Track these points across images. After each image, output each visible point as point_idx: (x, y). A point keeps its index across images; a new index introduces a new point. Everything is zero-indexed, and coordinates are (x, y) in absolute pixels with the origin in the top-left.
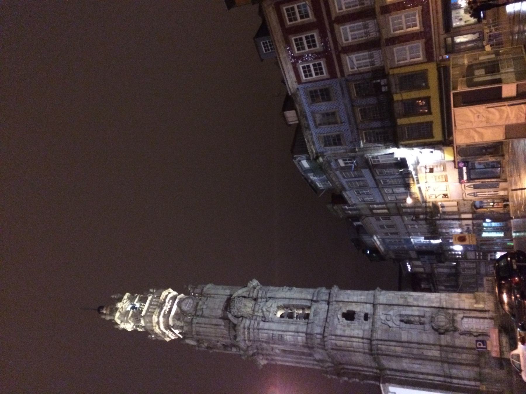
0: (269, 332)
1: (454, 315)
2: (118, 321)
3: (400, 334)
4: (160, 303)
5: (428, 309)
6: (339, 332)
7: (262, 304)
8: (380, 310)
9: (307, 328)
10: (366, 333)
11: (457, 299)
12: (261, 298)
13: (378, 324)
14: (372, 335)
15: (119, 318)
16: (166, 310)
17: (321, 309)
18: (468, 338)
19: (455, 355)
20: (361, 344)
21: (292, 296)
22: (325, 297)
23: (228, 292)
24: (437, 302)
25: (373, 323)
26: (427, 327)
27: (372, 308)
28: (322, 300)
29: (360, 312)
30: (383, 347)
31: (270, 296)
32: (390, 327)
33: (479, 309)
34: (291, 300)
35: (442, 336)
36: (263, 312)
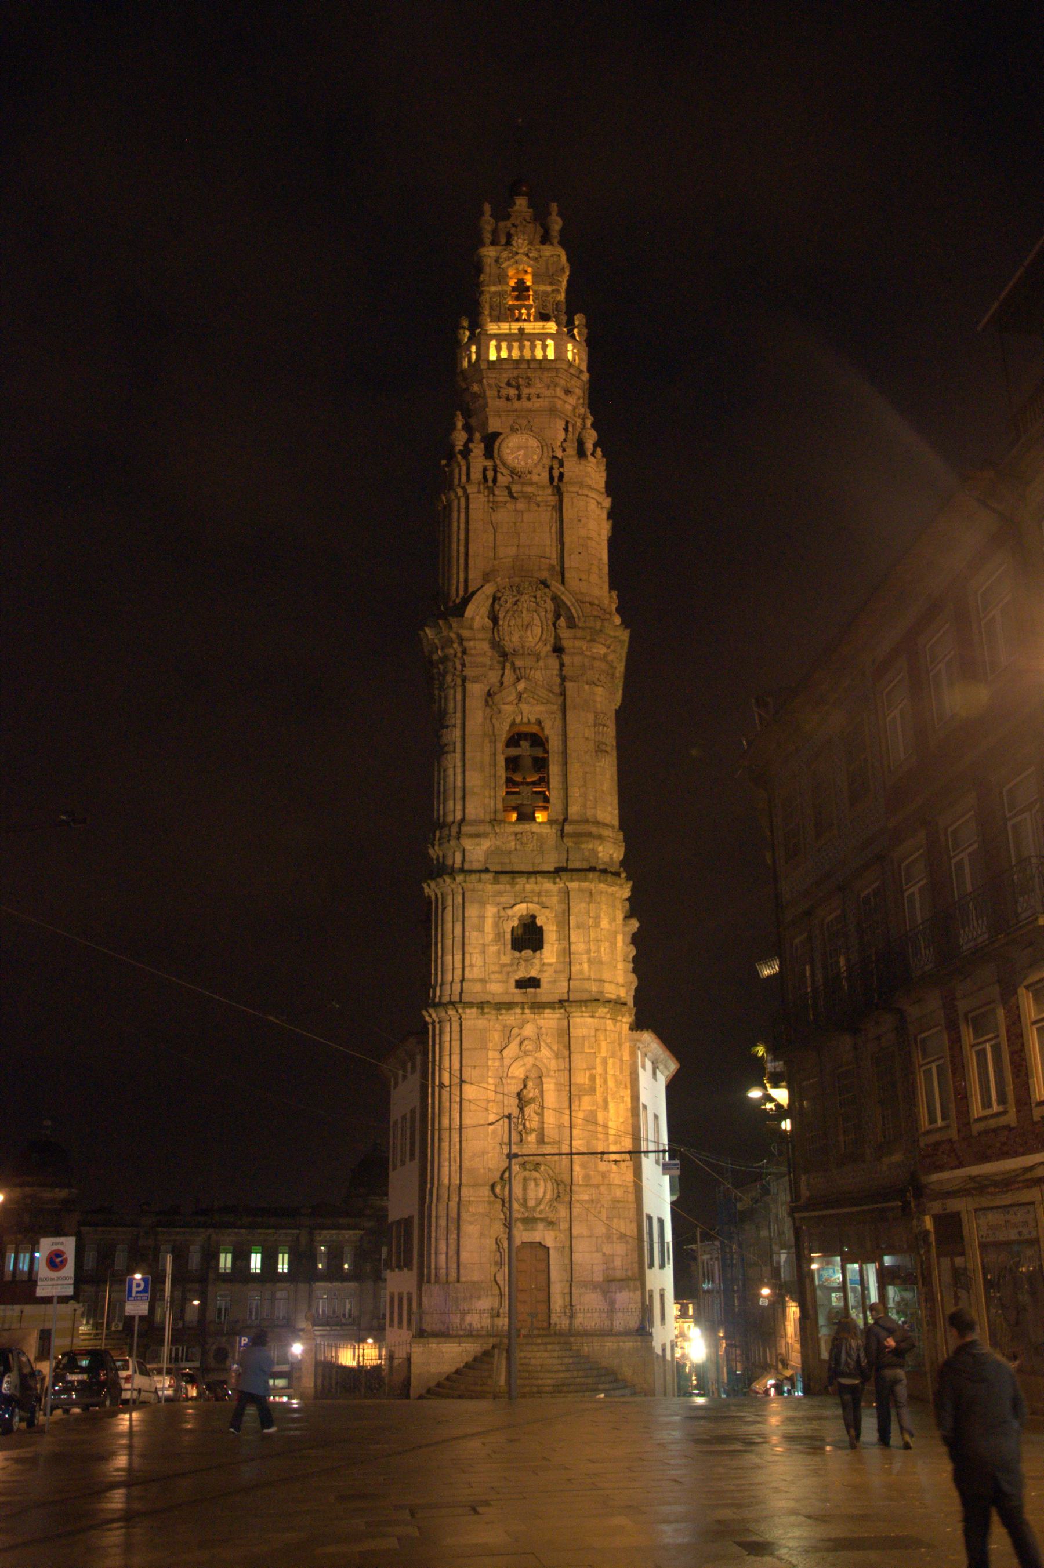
10: (478, 987)
11: (600, 1230)
14: (470, 1004)
19: (443, 1222)
24: (587, 1177)
30: (448, 1039)
35: (486, 1191)
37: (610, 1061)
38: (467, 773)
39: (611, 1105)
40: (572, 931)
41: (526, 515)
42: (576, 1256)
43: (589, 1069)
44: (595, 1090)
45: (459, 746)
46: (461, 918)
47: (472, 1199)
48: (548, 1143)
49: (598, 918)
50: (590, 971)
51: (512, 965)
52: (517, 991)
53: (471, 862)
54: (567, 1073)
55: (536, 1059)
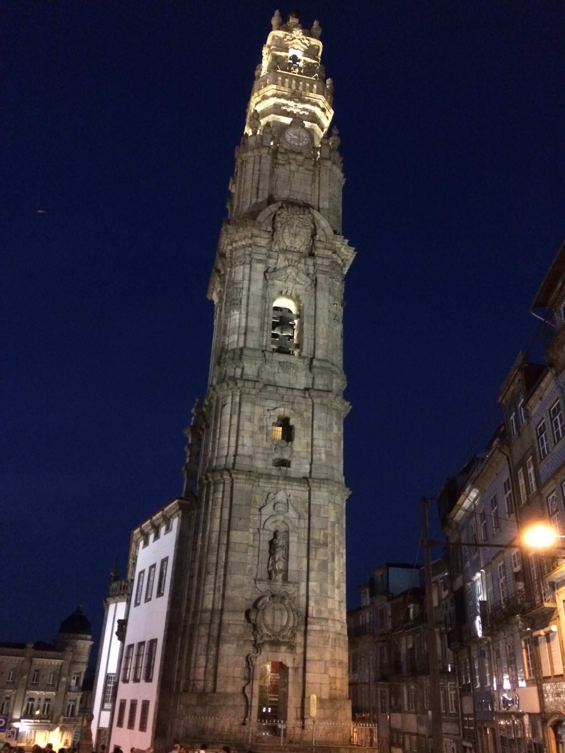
0: (246, 282)
1: (291, 647)
2: (269, 41)
3: (246, 528)
4: (301, 95)
5: (303, 591)
6: (246, 409)
7: (302, 266)
8: (298, 492)
9: (254, 350)
10: (247, 461)
11: (328, 656)
12: (314, 265)
13: (266, 486)
14: (240, 472)
15: (273, 38)
16: (288, 106)
17: (296, 376)
18: (239, 671)
19: (204, 640)
20: (225, 452)
21: (320, 319)
22: (320, 383)
23: (325, 204)
24: (319, 611)
25: (269, 476)
26: (263, 586)
27: (301, 476)
28: (314, 378)
29: (292, 451)
30: (220, 495)
31: (319, 281)
32: (260, 510)
33: (306, 706)
34: (312, 320)
35: (242, 617)
36: (285, 268)
37: (337, 525)
38: (249, 318)
39: (336, 558)
40: (314, 431)
41: (296, 174)
42: (309, 676)
43: (324, 529)
44: (327, 546)
45: (244, 301)
46: (237, 413)
47: (231, 622)
48: (290, 582)
49: (331, 425)
50: (326, 459)
51: (271, 449)
52: (274, 468)
53: (248, 375)
54: (306, 530)
55: (285, 517)
